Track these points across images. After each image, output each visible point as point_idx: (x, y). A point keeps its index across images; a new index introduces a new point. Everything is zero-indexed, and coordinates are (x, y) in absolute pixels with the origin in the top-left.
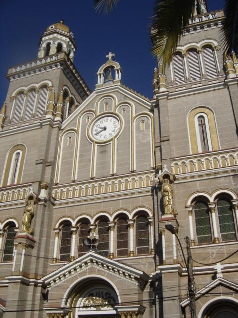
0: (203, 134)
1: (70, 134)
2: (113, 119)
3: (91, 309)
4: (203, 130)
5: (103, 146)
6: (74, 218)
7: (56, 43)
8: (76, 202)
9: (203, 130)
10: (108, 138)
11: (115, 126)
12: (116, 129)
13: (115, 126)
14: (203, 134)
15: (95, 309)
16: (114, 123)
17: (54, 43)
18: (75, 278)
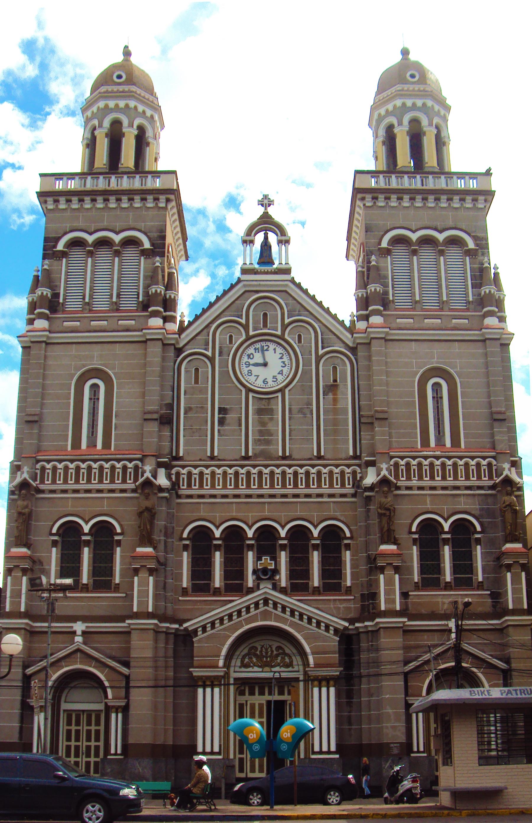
0: (438, 416)
1: (195, 364)
2: (279, 350)
3: (253, 670)
4: (438, 407)
5: (265, 400)
6: (217, 524)
7: (406, 120)
8: (220, 501)
9: (438, 407)
10: (272, 386)
11: (284, 362)
12: (286, 370)
13: (284, 362)
14: (438, 416)
15: (260, 670)
16: (281, 358)
17: (400, 124)
18: (285, 621)
